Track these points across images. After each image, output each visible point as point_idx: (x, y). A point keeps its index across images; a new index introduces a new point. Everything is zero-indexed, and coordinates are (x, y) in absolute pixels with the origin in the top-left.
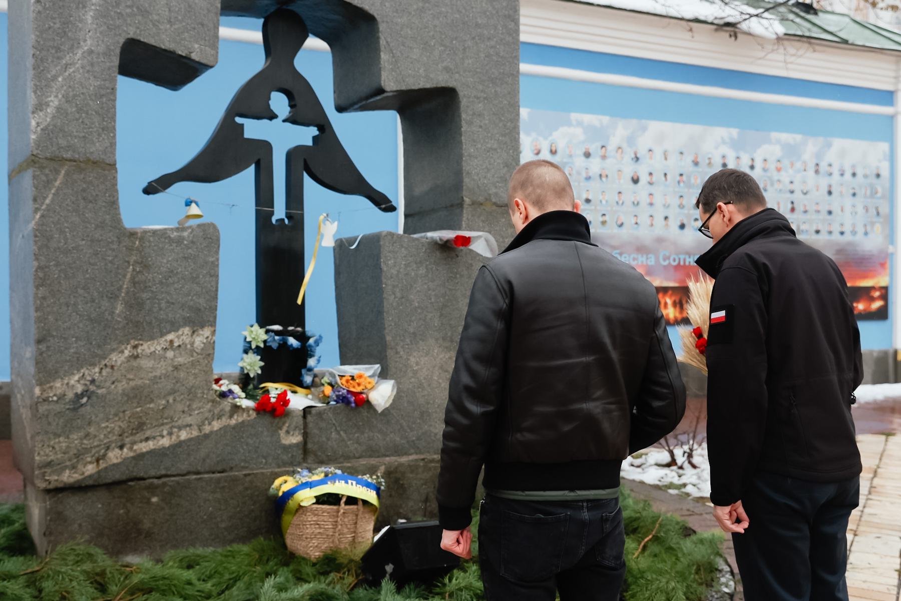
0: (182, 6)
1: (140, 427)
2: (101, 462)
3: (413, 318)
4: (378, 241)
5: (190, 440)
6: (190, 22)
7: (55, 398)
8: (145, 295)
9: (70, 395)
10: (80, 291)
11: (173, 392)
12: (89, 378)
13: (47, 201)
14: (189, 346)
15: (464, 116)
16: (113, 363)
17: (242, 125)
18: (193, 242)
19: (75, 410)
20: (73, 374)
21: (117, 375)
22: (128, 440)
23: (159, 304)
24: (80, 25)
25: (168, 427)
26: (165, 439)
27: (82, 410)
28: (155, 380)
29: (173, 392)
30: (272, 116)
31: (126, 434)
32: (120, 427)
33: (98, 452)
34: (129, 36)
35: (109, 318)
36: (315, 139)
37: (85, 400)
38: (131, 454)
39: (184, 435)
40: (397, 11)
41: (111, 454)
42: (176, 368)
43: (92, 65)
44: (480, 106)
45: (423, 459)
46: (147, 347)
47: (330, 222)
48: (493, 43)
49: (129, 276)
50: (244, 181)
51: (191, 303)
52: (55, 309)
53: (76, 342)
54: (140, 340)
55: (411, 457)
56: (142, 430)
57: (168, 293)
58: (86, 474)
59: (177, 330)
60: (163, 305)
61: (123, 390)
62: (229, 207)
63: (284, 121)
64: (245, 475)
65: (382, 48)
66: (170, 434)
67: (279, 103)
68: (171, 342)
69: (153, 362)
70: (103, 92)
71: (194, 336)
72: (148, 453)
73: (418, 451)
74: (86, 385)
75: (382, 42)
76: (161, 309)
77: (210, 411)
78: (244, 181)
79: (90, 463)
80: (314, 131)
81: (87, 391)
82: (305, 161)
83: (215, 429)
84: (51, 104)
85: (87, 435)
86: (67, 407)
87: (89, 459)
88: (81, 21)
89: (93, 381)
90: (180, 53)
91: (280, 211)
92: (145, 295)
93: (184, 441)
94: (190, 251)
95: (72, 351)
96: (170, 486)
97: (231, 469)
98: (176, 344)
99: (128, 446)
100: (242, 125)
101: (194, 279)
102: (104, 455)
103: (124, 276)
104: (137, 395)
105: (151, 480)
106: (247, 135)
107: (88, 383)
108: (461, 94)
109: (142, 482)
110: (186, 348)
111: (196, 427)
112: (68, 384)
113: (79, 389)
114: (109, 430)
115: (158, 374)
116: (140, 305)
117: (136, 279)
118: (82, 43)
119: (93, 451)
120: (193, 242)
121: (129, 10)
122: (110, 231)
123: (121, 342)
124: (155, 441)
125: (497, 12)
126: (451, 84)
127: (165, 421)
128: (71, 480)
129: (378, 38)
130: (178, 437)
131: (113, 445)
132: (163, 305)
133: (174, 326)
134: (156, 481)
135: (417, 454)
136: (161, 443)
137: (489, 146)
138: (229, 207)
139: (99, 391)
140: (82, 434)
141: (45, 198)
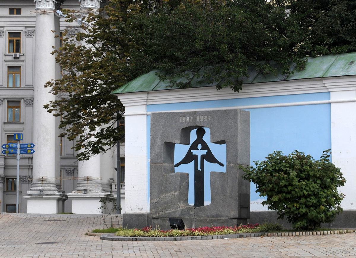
1: (166, 209)
8: (167, 186)
9: (155, 202)
17: (192, 152)
36: (207, 153)
39: (173, 211)
41: (161, 213)
42: (172, 198)
46: (167, 195)
50: (193, 163)
62: (189, 169)
67: (200, 146)
73: (217, 217)
78: (193, 163)
80: (207, 151)
91: (199, 168)
92: (167, 186)
100: (192, 152)
104: (165, 203)
106: (193, 154)
113: (156, 201)
116: (166, 187)
126: (224, 139)
138: (189, 169)
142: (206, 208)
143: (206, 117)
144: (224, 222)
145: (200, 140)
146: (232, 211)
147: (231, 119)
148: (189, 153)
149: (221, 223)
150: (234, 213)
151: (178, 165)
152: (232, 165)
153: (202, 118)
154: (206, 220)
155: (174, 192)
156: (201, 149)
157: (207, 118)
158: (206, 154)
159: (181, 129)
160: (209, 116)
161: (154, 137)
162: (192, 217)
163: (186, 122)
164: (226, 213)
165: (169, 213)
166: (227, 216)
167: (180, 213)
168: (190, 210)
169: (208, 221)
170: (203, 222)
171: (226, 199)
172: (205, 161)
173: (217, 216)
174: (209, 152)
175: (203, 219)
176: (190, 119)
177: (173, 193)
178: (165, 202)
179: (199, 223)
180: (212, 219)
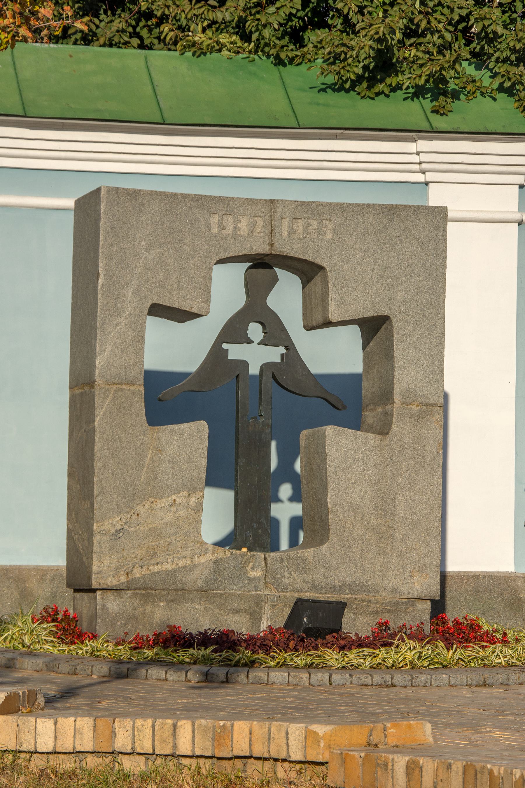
1: (154, 555)
2: (129, 575)
5: (185, 567)
7: (104, 532)
9: (113, 531)
11: (175, 534)
12: (124, 521)
13: (104, 409)
14: (186, 504)
20: (115, 517)
21: (140, 520)
23: (168, 475)
24: (125, 299)
26: (169, 565)
27: (120, 540)
29: (175, 534)
34: (154, 302)
36: (282, 356)
37: (121, 534)
38: (148, 572)
40: (343, 262)
41: (135, 571)
43: (131, 322)
45: (356, 599)
49: (149, 456)
53: (117, 497)
54: (155, 498)
58: (122, 581)
60: (170, 476)
63: (259, 344)
66: (172, 562)
67: (255, 331)
68: (175, 500)
69: (163, 513)
72: (158, 572)
74: (122, 525)
77: (199, 548)
81: (123, 529)
82: (273, 373)
83: (202, 561)
86: (111, 538)
87: (122, 573)
89: (126, 523)
98: (177, 503)
102: (132, 571)
103: (147, 456)
106: (231, 356)
108: (394, 320)
109: (154, 592)
110: (184, 506)
111: (189, 559)
112: (112, 523)
115: (165, 520)
121: (153, 285)
124: (163, 566)
127: (170, 553)
130: (177, 564)
131: (137, 565)
132: (170, 476)
135: (352, 594)
140: (119, 556)
141: (102, 408)
143: (315, 224)
149: (370, 613)
155: (185, 493)
156: (262, 343)
157: (320, 229)
163: (234, 236)
166: (395, 591)
167: (206, 572)
171: (390, 528)
174: (291, 355)
176: (252, 227)
177: (181, 497)
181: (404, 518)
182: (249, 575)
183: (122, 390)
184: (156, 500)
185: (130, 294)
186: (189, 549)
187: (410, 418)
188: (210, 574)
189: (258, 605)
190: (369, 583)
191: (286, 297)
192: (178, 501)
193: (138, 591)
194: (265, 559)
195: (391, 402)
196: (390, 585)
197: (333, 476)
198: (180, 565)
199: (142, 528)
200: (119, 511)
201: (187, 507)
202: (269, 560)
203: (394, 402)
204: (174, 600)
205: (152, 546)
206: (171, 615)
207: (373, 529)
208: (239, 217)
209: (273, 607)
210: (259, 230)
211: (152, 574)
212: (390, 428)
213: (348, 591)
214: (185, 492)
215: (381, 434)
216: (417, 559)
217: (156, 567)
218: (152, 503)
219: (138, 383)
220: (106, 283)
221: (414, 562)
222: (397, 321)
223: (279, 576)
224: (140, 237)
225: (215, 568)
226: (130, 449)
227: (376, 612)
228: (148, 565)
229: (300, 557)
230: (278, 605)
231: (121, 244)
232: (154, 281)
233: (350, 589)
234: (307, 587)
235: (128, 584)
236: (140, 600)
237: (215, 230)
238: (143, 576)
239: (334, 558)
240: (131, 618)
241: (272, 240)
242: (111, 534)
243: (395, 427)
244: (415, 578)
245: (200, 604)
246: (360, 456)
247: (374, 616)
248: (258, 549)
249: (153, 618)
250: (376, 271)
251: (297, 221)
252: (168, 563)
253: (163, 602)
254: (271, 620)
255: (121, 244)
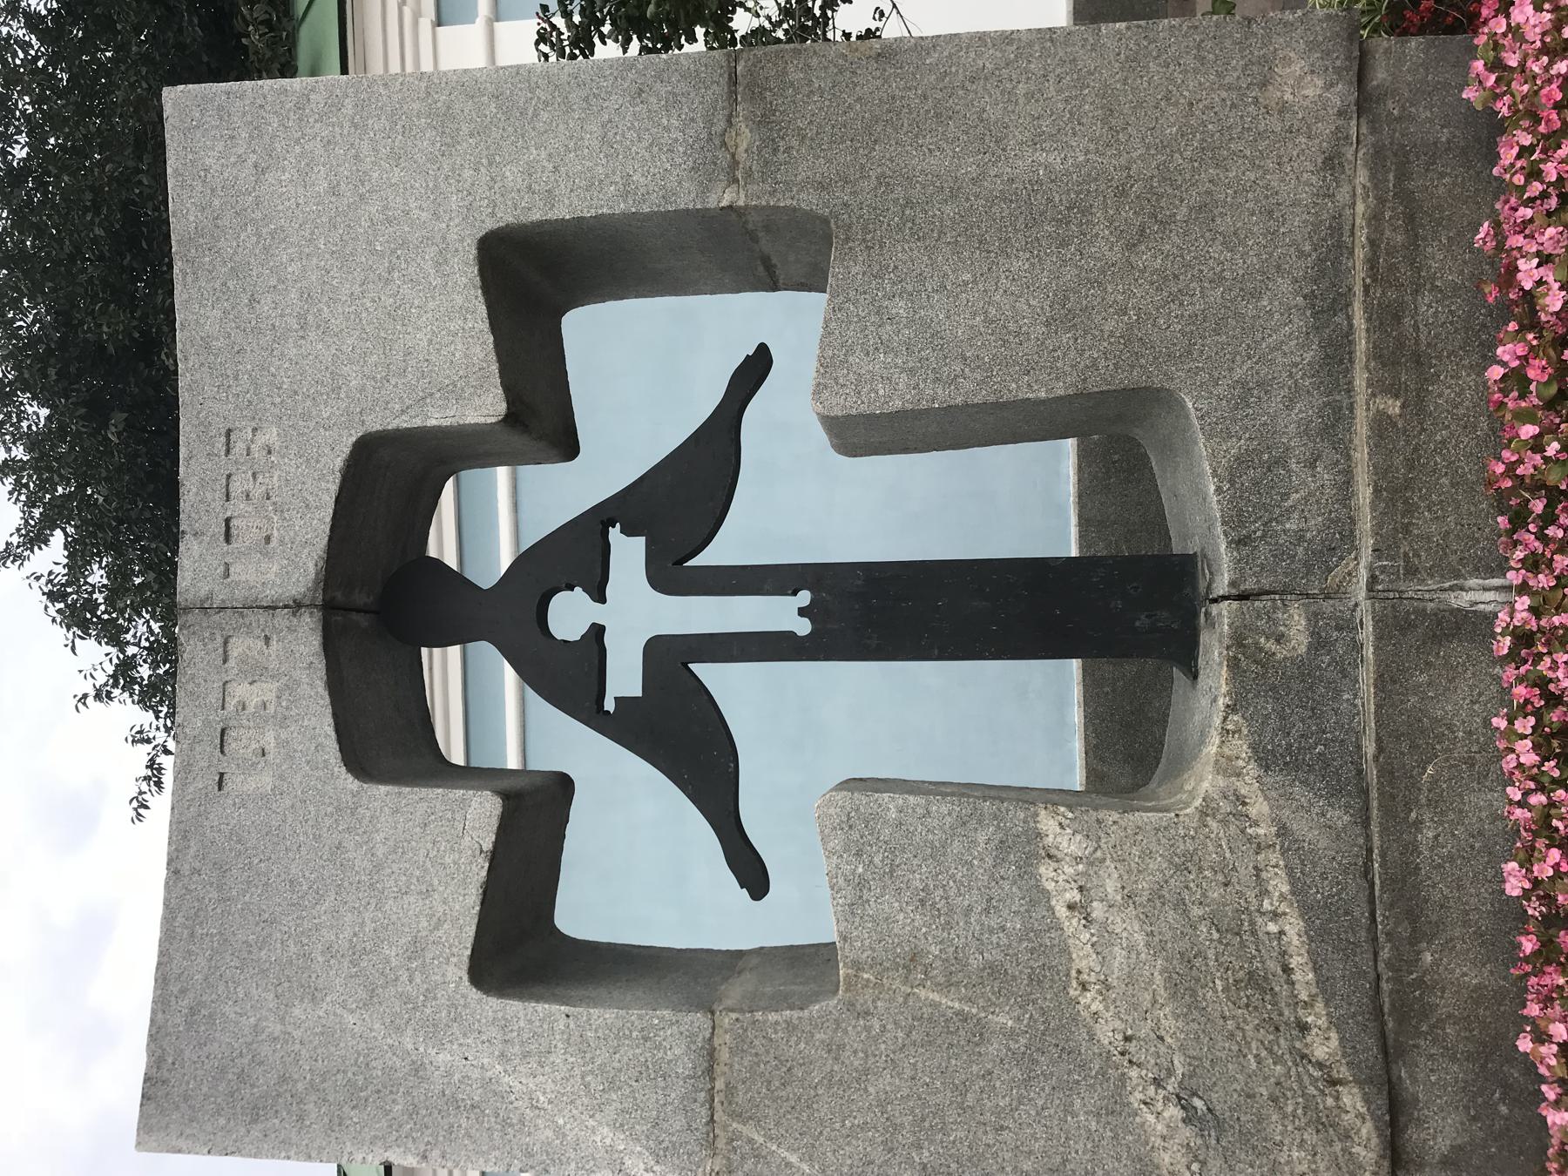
0: (395, 867)
1: (1256, 981)
2: (1335, 1074)
3: (1012, 326)
4: (836, 418)
5: (1290, 870)
6: (423, 852)
9: (1187, 1133)
10: (970, 1099)
11: (1181, 905)
13: (793, 1159)
15: (536, 216)
16: (1120, 1037)
17: (619, 700)
18: (859, 854)
19: (1220, 1125)
22: (1286, 1013)
23: (991, 932)
25: (1259, 920)
26: (1287, 928)
28: (1157, 947)
30: (597, 632)
31: (1275, 1016)
32: (1257, 1028)
33: (1314, 1080)
34: (466, 977)
35: (1023, 1041)
37: (1198, 1103)
38: (1320, 1006)
39: (1280, 885)
41: (1320, 1052)
43: (526, 1055)
44: (512, 175)
45: (1366, 288)
46: (1084, 959)
47: (803, 502)
48: (365, 147)
49: (935, 997)
51: (989, 861)
52: (1008, 1156)
54: (1068, 975)
55: (1359, 321)
56: (1265, 978)
57: (969, 910)
58: (1361, 1107)
59: (1045, 892)
60: (994, 922)
61: (1177, 1017)
64: (1380, 749)
65: (417, 422)
66: (1275, 916)
67: (569, 615)
68: (1071, 907)
70: (575, 1038)
71: (1060, 855)
72: (1315, 970)
73: (1341, 303)
75: (405, 422)
76: (1003, 929)
77: (1224, 822)
79: (1337, 1099)
81: (1179, 1098)
83: (1265, 809)
84: (608, 1141)
85: (1274, 1099)
87: (1330, 1101)
88: (448, 1074)
89: (1157, 1082)
90: (484, 873)
91: (783, 614)
92: (975, 961)
93: (1292, 884)
94: (877, 860)
95: (1093, 1126)
96: (1397, 924)
97: (1360, 772)
98: (1074, 896)
99: (1301, 1012)
100: (619, 700)
101: (937, 853)
102: (1320, 1065)
104: (1185, 985)
105: (1381, 966)
107: (1162, 1092)
108: (490, 225)
109: (1385, 986)
110: (1085, 874)
112: (1164, 1138)
113: (1174, 1112)
114: (1264, 1053)
115: (1140, 938)
116: (993, 970)
117: (941, 979)
118: (489, 1074)
119: (1312, 1090)
120: (859, 854)
122: (845, 1032)
123: (1074, 1019)
124: (1292, 950)
125: (297, 142)
128: (1375, 1141)
129: (397, 430)
130: (1282, 897)
131: (1298, 1045)
132: (994, 922)
133: (1039, 897)
134: (1385, 954)
135: (1349, 305)
136: (1296, 942)
137: (595, 143)
139: (1179, 1072)
141: (789, 1165)
142: (1234, 447)
144: (1405, 196)
145: (510, 616)
146: (1273, 94)
147: (259, 170)
148: (633, 727)
149: (1414, 241)
150: (1298, 67)
151: (752, 874)
152: (745, 138)
153: (248, 528)
154: (1381, 425)
155: (1045, 870)
156: (599, 596)
158: (643, 539)
159: (352, 783)
160: (239, 448)
161: (413, 1112)
162: (1348, 625)
163: (283, 722)
164: (1296, 181)
165: (1316, 935)
166: (1332, 162)
168: (1265, 661)
169: (1394, 407)
170: (1410, 465)
171: (1121, 192)
172: (714, 555)
173: (1327, 305)
175: (1381, 473)
178: (1173, 987)
179: (1424, 523)
180: (1376, 354)
181: (1092, 147)
182: (1303, 649)
183: (730, 1089)
184: (1073, 973)
185: (443, 1058)
186: (1228, 855)
187: (775, 151)
188: (1305, 783)
189: (1411, 626)
190: (1307, 248)
191: (489, 523)
192: (1074, 896)
193: (1390, 1042)
194: (1243, 597)
195: (734, 216)
196: (1314, 179)
197: (968, 385)
198: (1285, 888)
199: (1169, 1024)
200: (1115, 1108)
201: (1091, 864)
202: (1249, 585)
203: (730, 207)
204: (1412, 916)
205: (1226, 989)
206: (1466, 924)
207: (1131, 247)
208: (231, 703)
209: (1411, 572)
210: (260, 644)
211: (1324, 991)
212: (811, 216)
213: (1340, 318)
214: (1042, 870)
215: (828, 240)
216: (1224, 94)
217: (1297, 976)
218: (1084, 987)
219: (708, 1035)
220: (410, 1145)
221: (1233, 106)
222: (493, 214)
223: (1300, 550)
224: (282, 1020)
225: (1286, 764)
226: (914, 1065)
227: (1410, 219)
228: (1295, 1003)
229: (1232, 482)
230: (1406, 554)
231: (300, 1086)
232: (405, 978)
233: (1333, 310)
234: (1329, 455)
235: (1370, 1081)
236: (1420, 1035)
237: (265, 781)
238: (1337, 1023)
239: (1231, 370)
240: (1484, 1067)
241: (286, 607)
242: (1199, 1141)
243: (808, 201)
244: (1288, 97)
245: (1418, 823)
246: (900, 308)
247: (1422, 226)
248: (1188, 590)
249: (1478, 988)
250: (357, 290)
251: (234, 532)
252: (1282, 933)
253: (1419, 953)
254: (1457, 577)
255: (300, 1086)
